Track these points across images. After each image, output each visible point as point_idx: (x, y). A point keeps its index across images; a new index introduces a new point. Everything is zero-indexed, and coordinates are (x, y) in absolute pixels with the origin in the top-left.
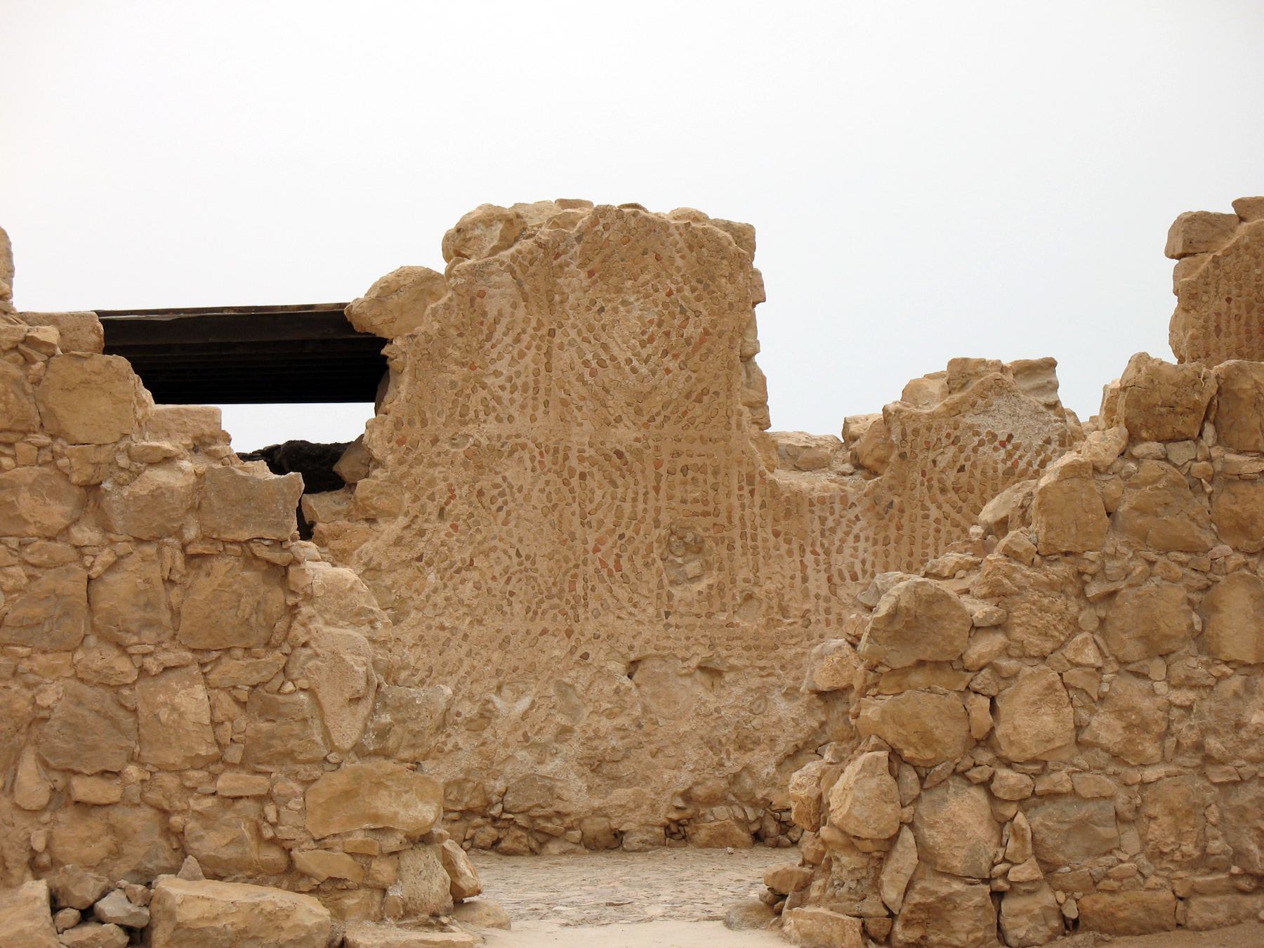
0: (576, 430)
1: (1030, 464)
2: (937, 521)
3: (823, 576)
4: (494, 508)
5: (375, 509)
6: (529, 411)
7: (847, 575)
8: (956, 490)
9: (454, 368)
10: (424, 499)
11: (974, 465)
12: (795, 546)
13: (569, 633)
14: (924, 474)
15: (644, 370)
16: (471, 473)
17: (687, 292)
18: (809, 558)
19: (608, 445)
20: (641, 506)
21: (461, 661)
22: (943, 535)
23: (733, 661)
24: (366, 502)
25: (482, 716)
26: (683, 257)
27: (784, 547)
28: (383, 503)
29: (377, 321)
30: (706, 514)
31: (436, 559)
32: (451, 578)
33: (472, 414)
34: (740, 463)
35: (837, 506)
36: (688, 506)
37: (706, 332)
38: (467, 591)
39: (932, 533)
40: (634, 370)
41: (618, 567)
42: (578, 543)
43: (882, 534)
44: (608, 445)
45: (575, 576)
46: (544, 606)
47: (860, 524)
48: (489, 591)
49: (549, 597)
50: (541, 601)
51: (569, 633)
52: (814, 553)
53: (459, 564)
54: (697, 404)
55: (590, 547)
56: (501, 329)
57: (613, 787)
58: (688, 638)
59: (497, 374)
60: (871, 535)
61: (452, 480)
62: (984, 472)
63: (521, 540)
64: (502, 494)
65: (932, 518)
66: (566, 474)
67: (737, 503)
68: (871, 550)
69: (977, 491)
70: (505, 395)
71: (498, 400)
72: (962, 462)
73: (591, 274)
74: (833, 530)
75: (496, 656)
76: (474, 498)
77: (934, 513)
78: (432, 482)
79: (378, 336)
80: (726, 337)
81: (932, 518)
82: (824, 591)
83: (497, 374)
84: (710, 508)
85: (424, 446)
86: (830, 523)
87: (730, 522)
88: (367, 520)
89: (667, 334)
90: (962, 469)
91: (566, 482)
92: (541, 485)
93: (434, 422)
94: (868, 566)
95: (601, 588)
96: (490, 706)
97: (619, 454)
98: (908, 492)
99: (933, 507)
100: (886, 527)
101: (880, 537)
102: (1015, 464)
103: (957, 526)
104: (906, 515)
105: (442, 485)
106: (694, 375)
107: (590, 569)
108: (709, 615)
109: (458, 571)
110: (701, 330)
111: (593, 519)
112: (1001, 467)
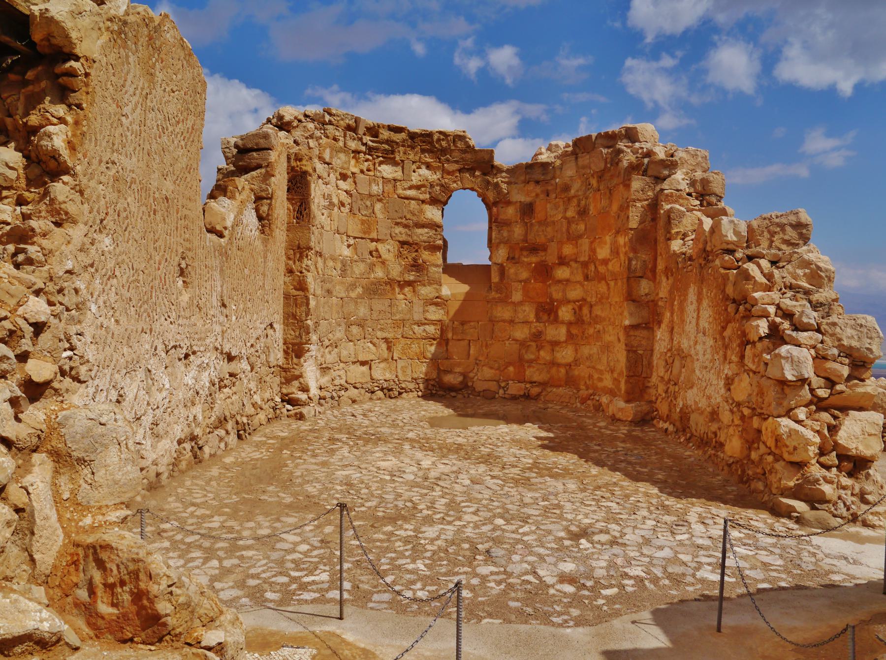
0: (153, 177)
5: (67, 213)
6: (137, 152)
9: (109, 100)
10: (95, 212)
13: (151, 330)
16: (116, 195)
19: (164, 192)
21: (112, 355)
23: (195, 348)
24: (63, 206)
25: (118, 402)
28: (72, 208)
29: (74, 35)
30: (190, 250)
31: (100, 268)
32: (106, 284)
33: (115, 147)
38: (113, 297)
42: (152, 262)
44: (164, 192)
46: (142, 310)
48: (121, 295)
49: (144, 302)
50: (141, 307)
51: (151, 330)
57: (158, 442)
59: (126, 116)
61: (107, 199)
64: (127, 218)
71: (126, 136)
75: (126, 350)
76: (116, 217)
78: (98, 197)
79: (66, 50)
83: (126, 116)
85: (95, 162)
88: (58, 224)
91: (149, 216)
92: (141, 215)
93: (100, 146)
95: (160, 295)
96: (122, 392)
97: (167, 198)
105: (103, 202)
107: (157, 282)
109: (109, 279)
111: (157, 244)
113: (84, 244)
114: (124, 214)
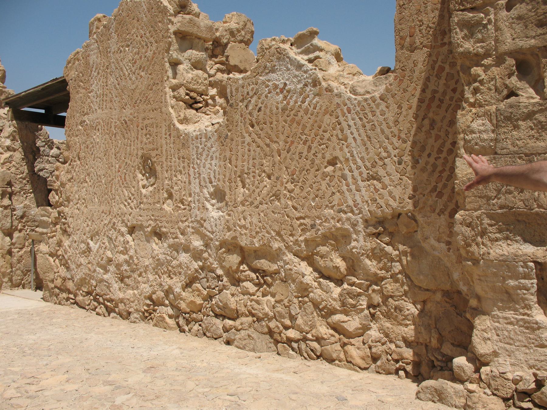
1: (296, 102)
2: (249, 144)
3: (197, 180)
4: (91, 153)
7: (207, 180)
8: (258, 124)
11: (266, 107)
12: (186, 164)
14: (242, 116)
15: (134, 78)
17: (148, 35)
18: (192, 172)
20: (132, 147)
22: (252, 153)
26: (146, 17)
27: (182, 165)
30: (153, 150)
34: (165, 120)
35: (204, 140)
36: (148, 146)
37: (154, 53)
39: (246, 150)
40: (131, 79)
41: (125, 178)
43: (223, 155)
45: (112, 185)
47: (214, 149)
52: (193, 168)
53: (82, 180)
54: (151, 92)
55: (117, 171)
56: (94, 69)
58: (147, 216)
60: (218, 156)
62: (271, 111)
63: (98, 168)
64: (93, 147)
65: (246, 143)
66: (111, 134)
67: (164, 142)
68: (218, 165)
69: (268, 124)
70: (95, 100)
72: (260, 105)
73: (118, 35)
74: (201, 155)
77: (248, 139)
80: (161, 53)
81: (246, 143)
82: (197, 190)
84: (155, 146)
86: (200, 150)
87: (162, 153)
89: (141, 58)
90: (260, 110)
94: (217, 173)
98: (234, 128)
99: (246, 135)
100: (225, 150)
101: (222, 157)
102: (288, 103)
103: (258, 147)
104: (234, 142)
106: (150, 76)
108: (154, 203)
109: (82, 184)
110: (152, 52)
112: (280, 106)
113: (68, 169)
114: (91, 146)
